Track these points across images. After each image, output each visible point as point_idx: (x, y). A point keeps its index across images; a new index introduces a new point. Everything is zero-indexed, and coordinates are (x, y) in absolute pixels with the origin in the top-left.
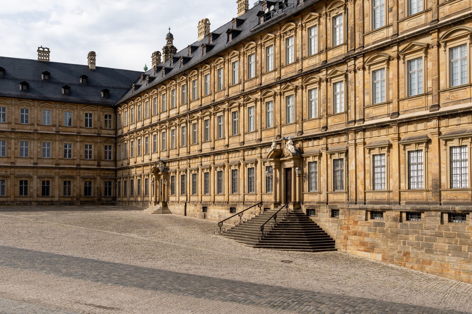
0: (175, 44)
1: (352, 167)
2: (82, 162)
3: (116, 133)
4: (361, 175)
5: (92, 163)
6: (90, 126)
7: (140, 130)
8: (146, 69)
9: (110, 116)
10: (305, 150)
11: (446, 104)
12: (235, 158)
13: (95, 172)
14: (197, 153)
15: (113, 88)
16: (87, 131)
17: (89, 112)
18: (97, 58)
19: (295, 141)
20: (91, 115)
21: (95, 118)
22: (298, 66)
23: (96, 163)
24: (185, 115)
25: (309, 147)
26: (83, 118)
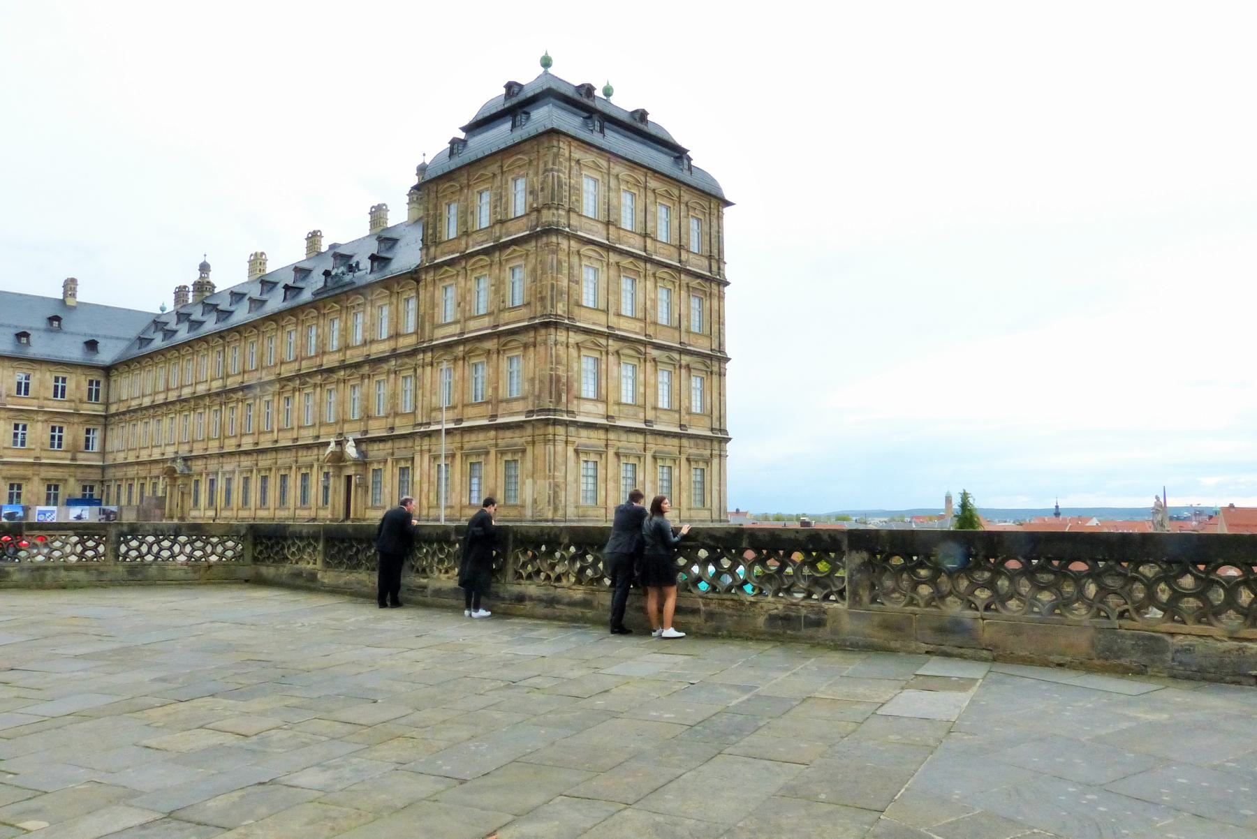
0: (213, 277)
1: (417, 478)
2: (44, 454)
3: (107, 410)
4: (425, 487)
5: (63, 455)
6: (63, 396)
7: (146, 408)
8: (162, 309)
9: (98, 383)
10: (371, 454)
11: (503, 416)
12: (284, 459)
13: (66, 470)
14: (233, 449)
15: (105, 337)
16: (56, 404)
17: (61, 375)
18: (78, 288)
19: (358, 442)
20: (64, 380)
21: (71, 385)
22: (365, 350)
23: (69, 455)
24: (218, 394)
25: (376, 451)
26: (53, 383)
